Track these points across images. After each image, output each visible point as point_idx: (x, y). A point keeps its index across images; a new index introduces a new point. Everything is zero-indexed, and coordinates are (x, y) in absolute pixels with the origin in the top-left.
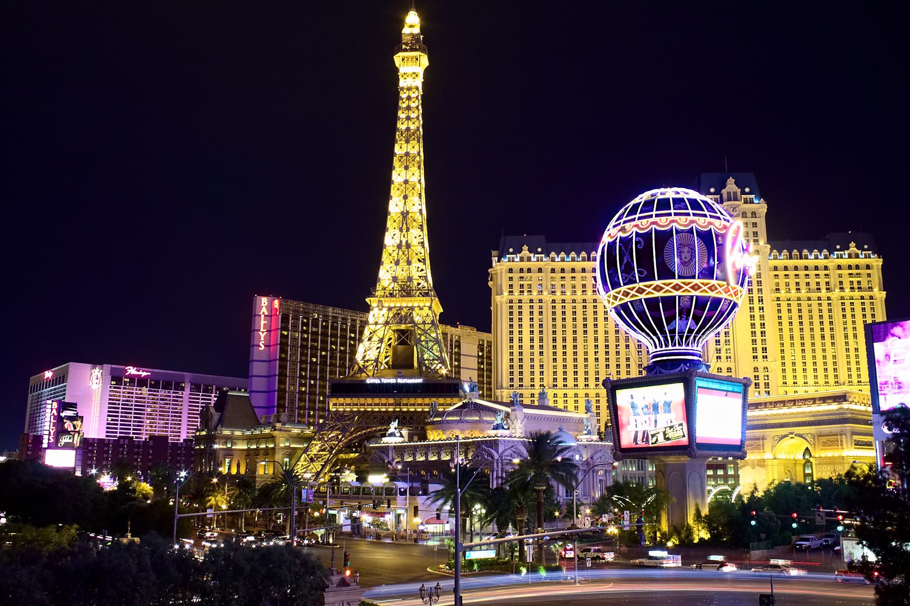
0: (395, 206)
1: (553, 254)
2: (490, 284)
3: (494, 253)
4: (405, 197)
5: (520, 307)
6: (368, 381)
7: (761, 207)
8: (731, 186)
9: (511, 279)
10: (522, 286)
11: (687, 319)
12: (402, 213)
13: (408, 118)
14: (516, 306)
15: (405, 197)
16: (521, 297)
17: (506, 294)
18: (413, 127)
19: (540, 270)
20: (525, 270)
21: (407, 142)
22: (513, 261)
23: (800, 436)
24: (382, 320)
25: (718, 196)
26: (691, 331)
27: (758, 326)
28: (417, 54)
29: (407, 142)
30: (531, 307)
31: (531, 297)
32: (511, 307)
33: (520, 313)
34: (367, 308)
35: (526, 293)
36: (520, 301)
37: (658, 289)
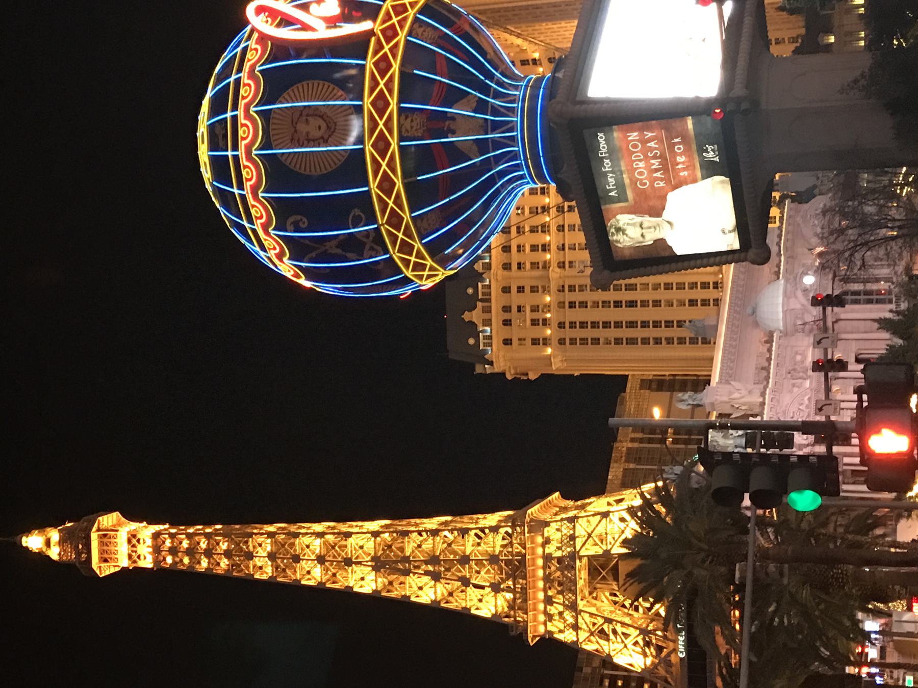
0: (364, 581)
2: (532, 376)
3: (479, 369)
5: (572, 325)
10: (534, 322)
11: (453, 117)
12: (376, 569)
13: (209, 553)
14: (568, 333)
15: (348, 562)
16: (555, 325)
17: (549, 351)
19: (506, 290)
20: (507, 316)
21: (250, 556)
22: (490, 337)
24: (569, 616)
26: (481, 107)
28: (94, 536)
30: (572, 305)
31: (554, 307)
32: (573, 341)
33: (583, 325)
34: (548, 642)
35: (548, 315)
37: (387, 185)
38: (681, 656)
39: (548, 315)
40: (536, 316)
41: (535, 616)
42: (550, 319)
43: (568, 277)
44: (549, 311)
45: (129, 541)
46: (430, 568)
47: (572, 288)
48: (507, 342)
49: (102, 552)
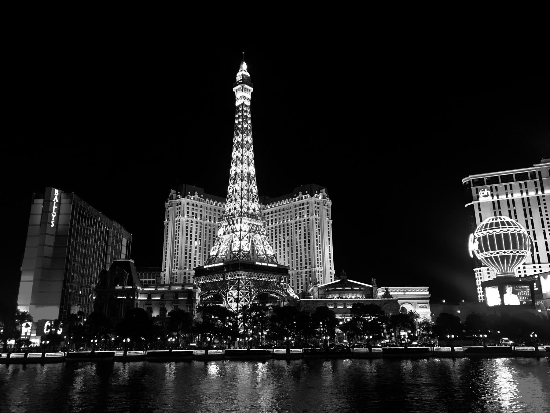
1: (207, 200)
4: (249, 165)
5: (192, 225)
6: (257, 263)
7: (330, 203)
8: (324, 190)
9: (188, 208)
10: (193, 213)
14: (190, 223)
17: (186, 216)
18: (249, 128)
23: (409, 303)
27: (307, 253)
29: (248, 135)
31: (196, 220)
32: (187, 224)
33: (191, 228)
36: (192, 222)
47: (201, 227)
48: (188, 204)
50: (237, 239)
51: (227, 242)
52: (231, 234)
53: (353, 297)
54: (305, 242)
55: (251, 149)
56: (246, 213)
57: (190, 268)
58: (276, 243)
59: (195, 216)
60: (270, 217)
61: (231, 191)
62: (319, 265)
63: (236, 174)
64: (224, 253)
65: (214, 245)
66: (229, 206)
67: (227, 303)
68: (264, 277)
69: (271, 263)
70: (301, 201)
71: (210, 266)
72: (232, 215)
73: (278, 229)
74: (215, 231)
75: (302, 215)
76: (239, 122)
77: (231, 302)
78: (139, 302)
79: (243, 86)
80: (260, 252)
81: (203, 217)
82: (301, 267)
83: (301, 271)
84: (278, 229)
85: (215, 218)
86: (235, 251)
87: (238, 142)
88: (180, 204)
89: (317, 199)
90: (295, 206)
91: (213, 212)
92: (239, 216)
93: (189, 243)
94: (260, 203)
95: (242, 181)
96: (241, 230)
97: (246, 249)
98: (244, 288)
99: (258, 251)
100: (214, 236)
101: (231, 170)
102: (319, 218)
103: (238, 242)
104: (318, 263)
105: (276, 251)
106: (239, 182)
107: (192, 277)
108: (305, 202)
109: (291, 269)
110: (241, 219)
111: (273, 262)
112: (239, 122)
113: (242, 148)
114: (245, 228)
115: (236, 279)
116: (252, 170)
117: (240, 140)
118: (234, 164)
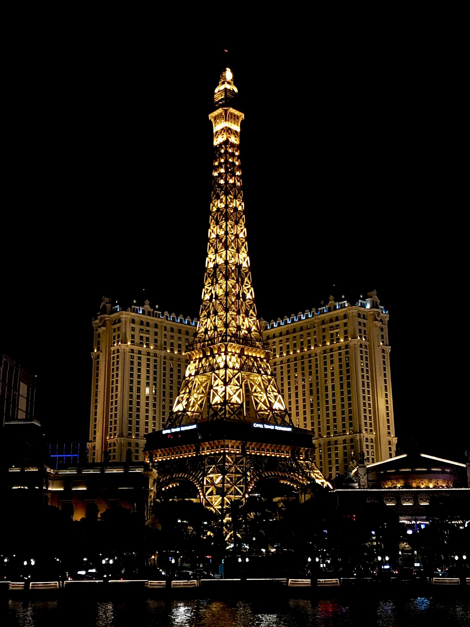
1: (166, 313)
4: (238, 251)
5: (140, 358)
6: (256, 425)
9: (133, 329)
10: (141, 338)
14: (136, 356)
17: (129, 343)
18: (238, 184)
20: (145, 323)
25: (365, 302)
27: (346, 406)
29: (235, 197)
32: (132, 357)
33: (139, 364)
36: (140, 352)
38: (254, 424)
39: (145, 346)
40: (144, 339)
41: (234, 347)
42: (143, 347)
43: (161, 360)
44: (147, 347)
45: (236, 132)
46: (241, 296)
47: (155, 361)
49: (231, 114)
50: (219, 381)
51: (202, 388)
52: (209, 374)
53: (431, 485)
54: (342, 386)
55: (242, 222)
56: (235, 336)
57: (137, 435)
58: (289, 389)
59: (144, 341)
60: (277, 343)
61: (207, 297)
62: (369, 428)
63: (216, 266)
64: (197, 406)
65: (179, 394)
66: (205, 324)
67: (204, 495)
68: (268, 450)
69: (280, 425)
70: (333, 313)
71: (173, 430)
72: (210, 339)
73: (292, 364)
74: (182, 368)
75: (335, 338)
76: (220, 174)
77: (211, 494)
78: (49, 495)
79: (226, 111)
80: (261, 405)
81: (159, 344)
82: (335, 432)
83: (335, 438)
84: (292, 364)
85: (180, 346)
86: (216, 404)
87: (218, 209)
88: (119, 321)
89: (362, 309)
90: (323, 323)
91: (176, 335)
92: (222, 341)
93: (135, 389)
94: (258, 317)
95: (227, 279)
96: (226, 367)
97: (235, 399)
98: (233, 469)
99: (257, 404)
100: (179, 377)
101: (207, 259)
102: (367, 343)
103: (220, 389)
104: (366, 423)
105: (290, 403)
106: (222, 281)
107: (141, 450)
108: (342, 315)
109: (316, 435)
110: (226, 346)
111: (284, 424)
112: (220, 174)
113: (226, 220)
114: (234, 362)
115: (220, 454)
116: (244, 259)
117: (223, 206)
118: (212, 249)
